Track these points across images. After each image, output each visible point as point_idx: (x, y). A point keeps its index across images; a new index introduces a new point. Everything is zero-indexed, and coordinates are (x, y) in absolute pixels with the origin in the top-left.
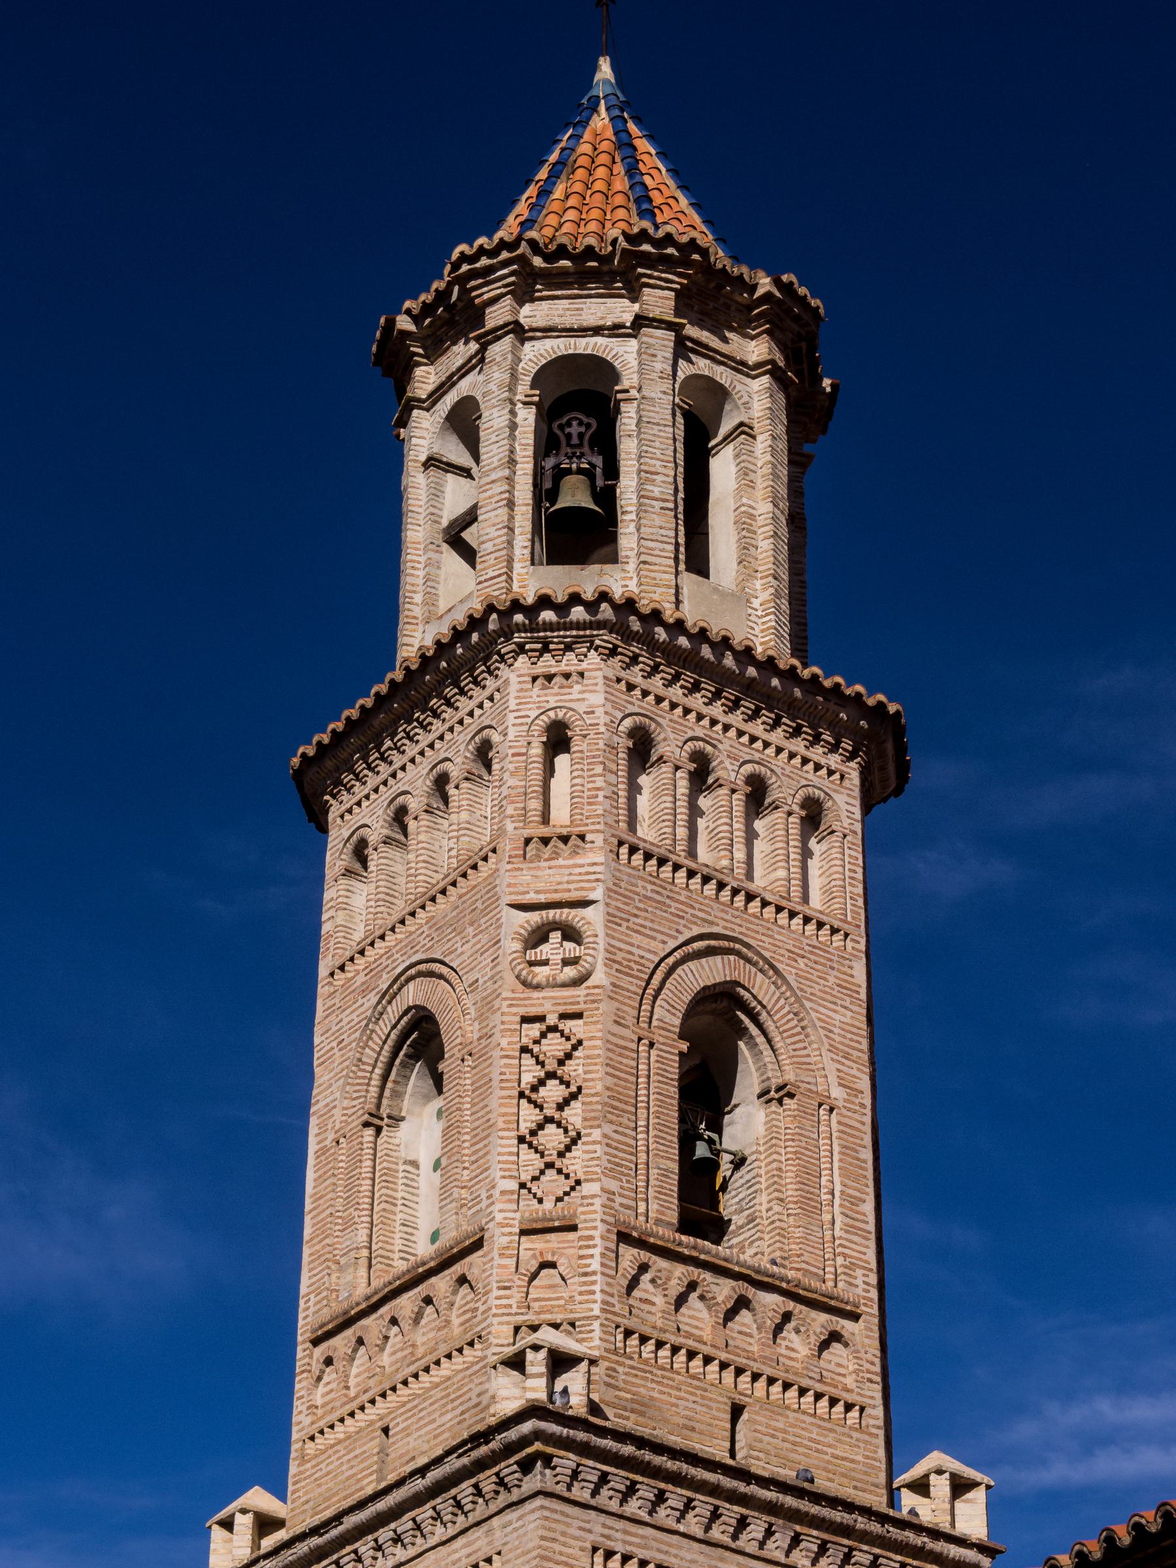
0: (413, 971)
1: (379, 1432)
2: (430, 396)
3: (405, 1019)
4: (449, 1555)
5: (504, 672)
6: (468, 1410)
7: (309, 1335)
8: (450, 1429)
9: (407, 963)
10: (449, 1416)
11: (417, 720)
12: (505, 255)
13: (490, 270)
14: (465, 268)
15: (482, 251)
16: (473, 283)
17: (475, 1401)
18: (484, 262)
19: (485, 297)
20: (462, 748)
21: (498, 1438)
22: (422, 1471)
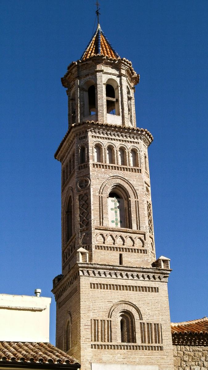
0: (119, 177)
1: (119, 254)
2: (105, 72)
3: (116, 184)
4: (144, 283)
5: (139, 141)
6: (145, 261)
7: (95, 227)
8: (140, 262)
9: (118, 175)
10: (139, 260)
11: (118, 134)
12: (128, 65)
13: (126, 65)
14: (123, 61)
15: (127, 62)
16: (122, 64)
17: (146, 260)
18: (126, 63)
19: (123, 68)
20: (129, 146)
21: (162, 271)
22: (143, 268)
